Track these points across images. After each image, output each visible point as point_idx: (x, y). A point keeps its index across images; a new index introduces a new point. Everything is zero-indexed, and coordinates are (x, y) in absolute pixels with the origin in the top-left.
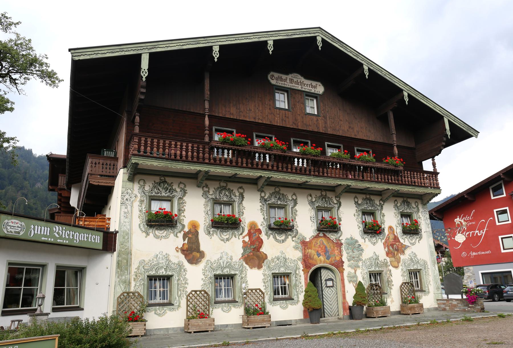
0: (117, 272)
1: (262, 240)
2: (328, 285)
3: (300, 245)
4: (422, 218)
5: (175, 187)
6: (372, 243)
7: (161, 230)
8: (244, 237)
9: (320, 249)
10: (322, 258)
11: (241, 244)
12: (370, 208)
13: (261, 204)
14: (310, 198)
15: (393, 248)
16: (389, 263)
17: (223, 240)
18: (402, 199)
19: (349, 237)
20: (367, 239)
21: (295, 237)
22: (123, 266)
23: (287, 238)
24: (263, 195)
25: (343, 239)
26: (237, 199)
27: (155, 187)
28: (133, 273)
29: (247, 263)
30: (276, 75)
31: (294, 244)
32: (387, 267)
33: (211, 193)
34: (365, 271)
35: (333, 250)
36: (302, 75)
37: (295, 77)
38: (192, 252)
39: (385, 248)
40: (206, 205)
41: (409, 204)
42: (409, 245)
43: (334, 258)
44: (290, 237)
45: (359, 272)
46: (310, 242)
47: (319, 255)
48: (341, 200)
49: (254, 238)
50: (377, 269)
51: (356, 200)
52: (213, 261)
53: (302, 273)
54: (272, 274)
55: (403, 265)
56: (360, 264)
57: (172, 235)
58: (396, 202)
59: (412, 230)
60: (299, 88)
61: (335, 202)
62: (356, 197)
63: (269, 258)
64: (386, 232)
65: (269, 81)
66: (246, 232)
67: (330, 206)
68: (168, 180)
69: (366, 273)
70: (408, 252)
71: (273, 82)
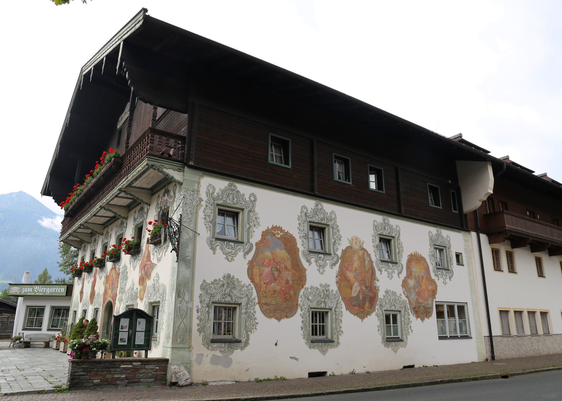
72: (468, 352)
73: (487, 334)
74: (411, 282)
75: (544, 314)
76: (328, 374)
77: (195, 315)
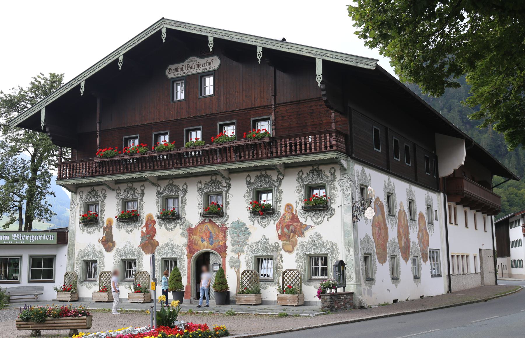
0: (68, 258)
1: (155, 229)
2: (214, 270)
3: (186, 232)
4: (339, 188)
5: (100, 193)
6: (261, 225)
7: (91, 227)
8: (142, 228)
9: (204, 235)
10: (205, 243)
11: (140, 234)
12: (265, 186)
13: (156, 198)
14: (199, 185)
15: (288, 229)
16: (281, 247)
17: (127, 232)
18: (311, 168)
19: (236, 220)
20: (256, 222)
21: (182, 224)
22: (71, 254)
23: (175, 226)
24: (159, 189)
25: (229, 223)
26: (139, 196)
27: (88, 195)
28: (75, 259)
29: (143, 250)
30: (173, 67)
31: (181, 231)
32: (277, 251)
33: (122, 194)
34: (250, 256)
35: (218, 235)
36: (197, 56)
37: (191, 62)
38: (108, 242)
39: (278, 230)
40: (118, 204)
41: (319, 173)
42: (312, 224)
43: (217, 243)
44: (178, 225)
45: (242, 258)
46: (196, 228)
47: (203, 240)
48: (231, 183)
49: (149, 229)
50: (265, 254)
51: (248, 179)
52: (120, 249)
53: (186, 258)
54: (162, 258)
55: (300, 249)
56: (245, 248)
57: (97, 230)
58: (301, 174)
59: (318, 206)
60: (194, 71)
61: (225, 185)
62: (249, 176)
63: (160, 245)
64: (282, 211)
65: (166, 76)
66: (144, 223)
67: (219, 190)
68: (96, 188)
69: (251, 258)
70: (308, 234)
71: (170, 76)
72: (437, 287)
73: (447, 274)
74: (421, 235)
75: (467, 256)
76: (399, 301)
77: (360, 262)
